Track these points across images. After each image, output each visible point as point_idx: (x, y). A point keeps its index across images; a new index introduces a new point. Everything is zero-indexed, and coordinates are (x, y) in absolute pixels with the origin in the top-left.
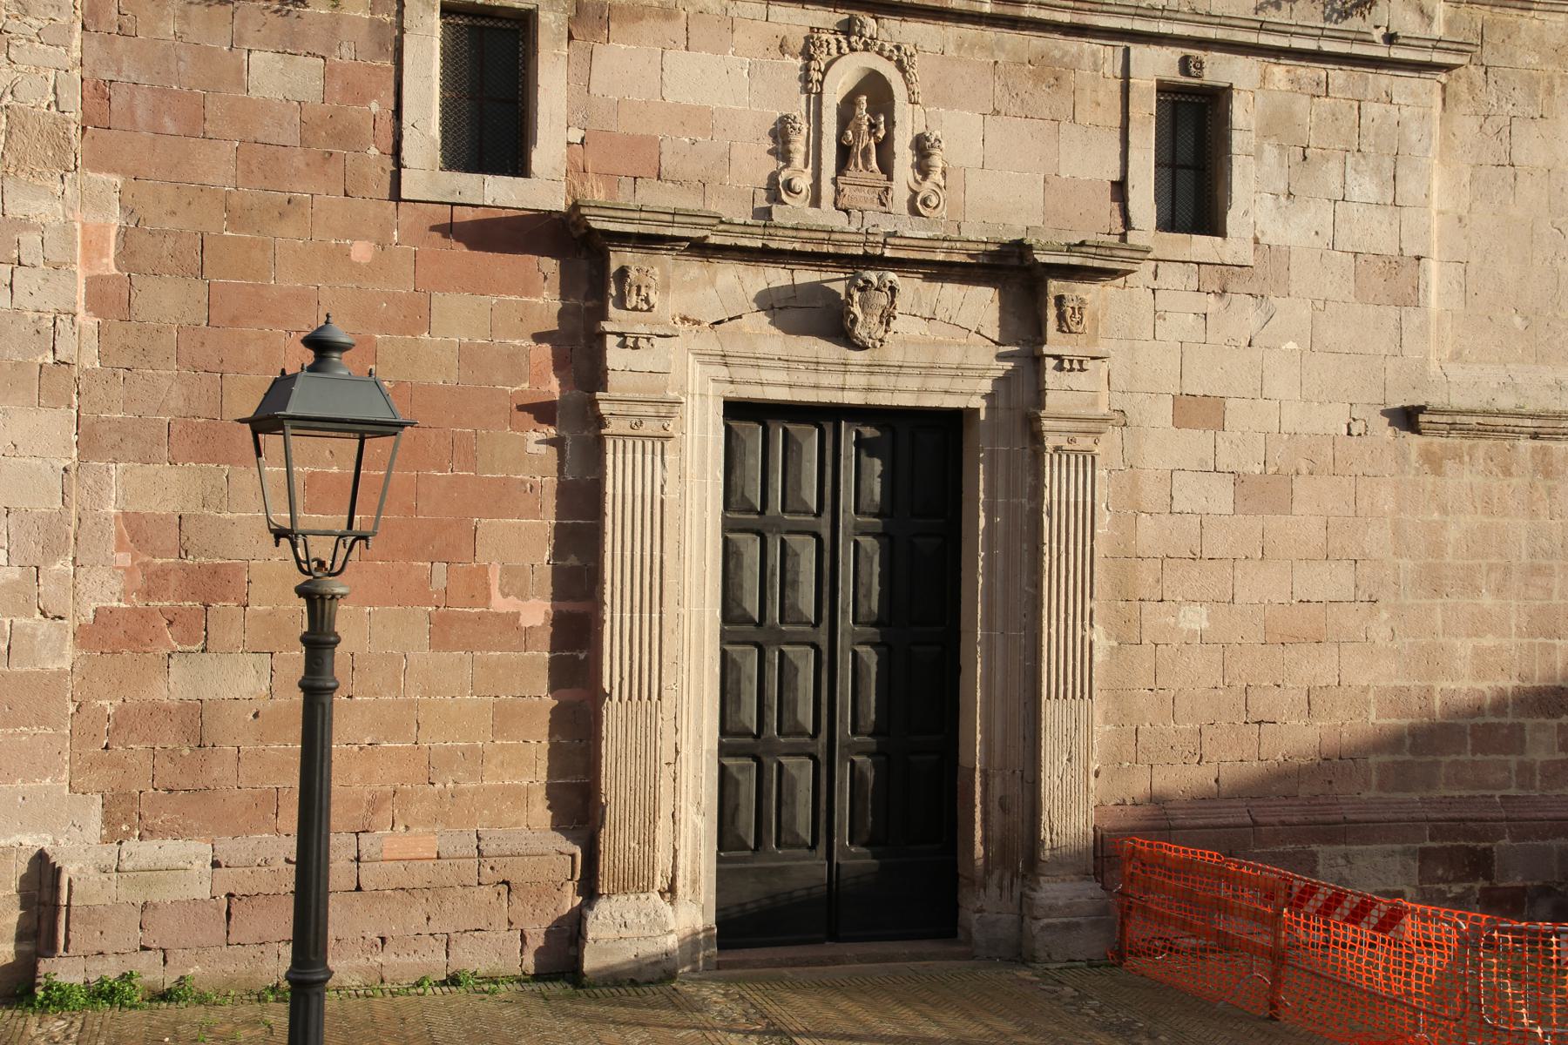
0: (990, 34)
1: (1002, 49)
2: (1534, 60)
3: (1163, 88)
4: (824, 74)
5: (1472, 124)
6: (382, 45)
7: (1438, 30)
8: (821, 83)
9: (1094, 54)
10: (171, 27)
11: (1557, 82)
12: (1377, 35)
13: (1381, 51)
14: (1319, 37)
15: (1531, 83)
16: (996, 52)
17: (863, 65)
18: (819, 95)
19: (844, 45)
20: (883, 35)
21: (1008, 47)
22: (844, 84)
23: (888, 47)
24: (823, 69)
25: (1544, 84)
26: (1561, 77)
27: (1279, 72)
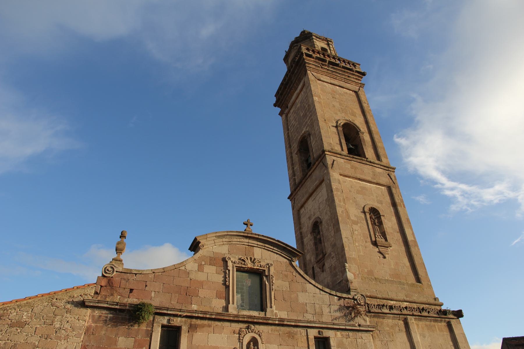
0: (278, 328)
1: (281, 331)
2: (388, 329)
3: (315, 338)
4: (243, 338)
5: (379, 343)
6: (148, 335)
7: (368, 323)
8: (243, 340)
9: (300, 331)
10: (103, 332)
11: (394, 333)
12: (357, 325)
13: (358, 328)
14: (345, 326)
15: (389, 333)
16: (280, 332)
17: (251, 335)
18: (242, 342)
19: (247, 331)
20: (255, 329)
21: (282, 330)
22: (247, 340)
23: (256, 331)
24: (243, 337)
25: (391, 334)
26: (394, 332)
27: (339, 333)
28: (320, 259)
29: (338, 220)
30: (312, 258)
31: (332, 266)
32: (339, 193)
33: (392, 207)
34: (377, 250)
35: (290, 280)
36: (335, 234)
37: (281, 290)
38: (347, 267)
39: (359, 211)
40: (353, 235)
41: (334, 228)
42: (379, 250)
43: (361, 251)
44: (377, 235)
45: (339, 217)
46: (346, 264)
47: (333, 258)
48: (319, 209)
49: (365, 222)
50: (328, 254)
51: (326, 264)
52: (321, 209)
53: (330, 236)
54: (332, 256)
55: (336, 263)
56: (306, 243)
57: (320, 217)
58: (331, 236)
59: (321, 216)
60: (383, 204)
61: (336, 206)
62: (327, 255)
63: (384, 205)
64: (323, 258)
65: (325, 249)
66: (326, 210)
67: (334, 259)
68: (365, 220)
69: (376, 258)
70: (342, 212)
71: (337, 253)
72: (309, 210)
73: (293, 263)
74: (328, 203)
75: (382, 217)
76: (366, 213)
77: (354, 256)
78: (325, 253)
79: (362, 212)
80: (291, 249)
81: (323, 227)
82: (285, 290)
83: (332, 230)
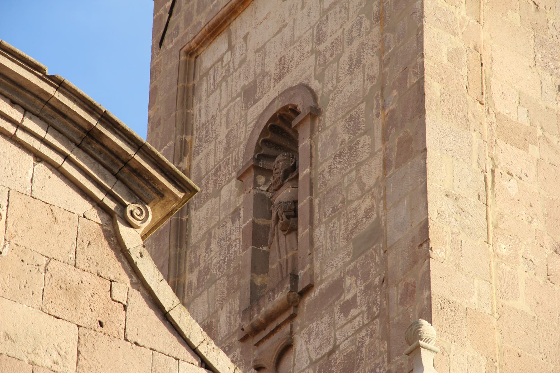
28: (270, 318)
29: (424, 95)
30: (223, 316)
31: (337, 354)
35: (90, 319)
36: (385, 173)
37: (23, 357)
38: (427, 341)
40: (490, 192)
41: (385, 138)
45: (427, 78)
46: (424, 322)
47: (346, 308)
48: (319, 39)
50: (323, 286)
51: (300, 344)
52: (327, 43)
53: (355, 187)
54: (349, 296)
55: (364, 333)
56: (202, 232)
57: (315, 85)
58: (362, 185)
59: (320, 78)
61: (422, 16)
62: (315, 293)
64: (292, 311)
65: (312, 262)
66: (356, 44)
67: (354, 312)
70: (451, 58)
71: (377, 281)
72: (257, 51)
73: (123, 229)
74: (375, 8)
77: (475, 299)
78: (306, 284)
80: (131, 152)
81: (323, 137)
82: (48, 362)
83: (372, 154)
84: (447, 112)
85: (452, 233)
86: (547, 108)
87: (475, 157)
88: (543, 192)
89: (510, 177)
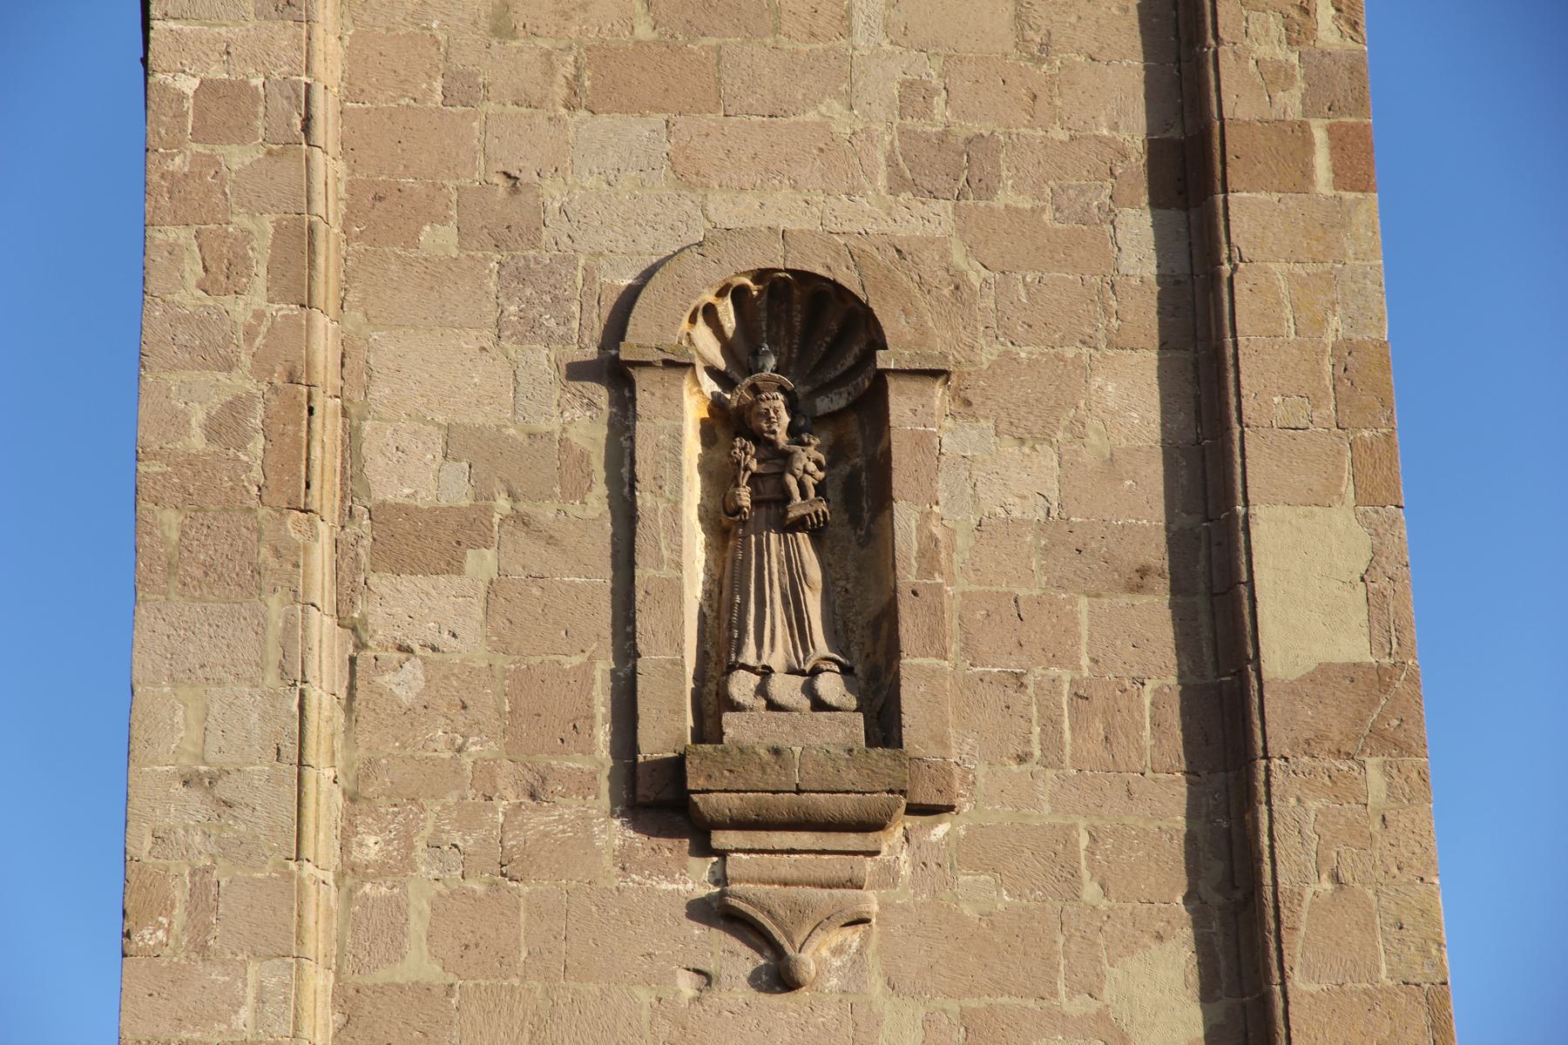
32: (238, 157)
33: (1157, 202)
34: (696, 880)
39: (543, 361)
42: (721, 879)
43: (417, 926)
44: (766, 672)
49: (597, 503)
60: (987, 190)
63: (1005, 197)
68: (600, 473)
69: (644, 996)
70: (213, 430)
75: (902, 405)
76: (642, 378)
77: (245, 1014)
79: (577, 372)
84: (198, 573)
85: (192, 874)
86: (530, 435)
87: (274, 655)
88: (501, 661)
89: (403, 656)
